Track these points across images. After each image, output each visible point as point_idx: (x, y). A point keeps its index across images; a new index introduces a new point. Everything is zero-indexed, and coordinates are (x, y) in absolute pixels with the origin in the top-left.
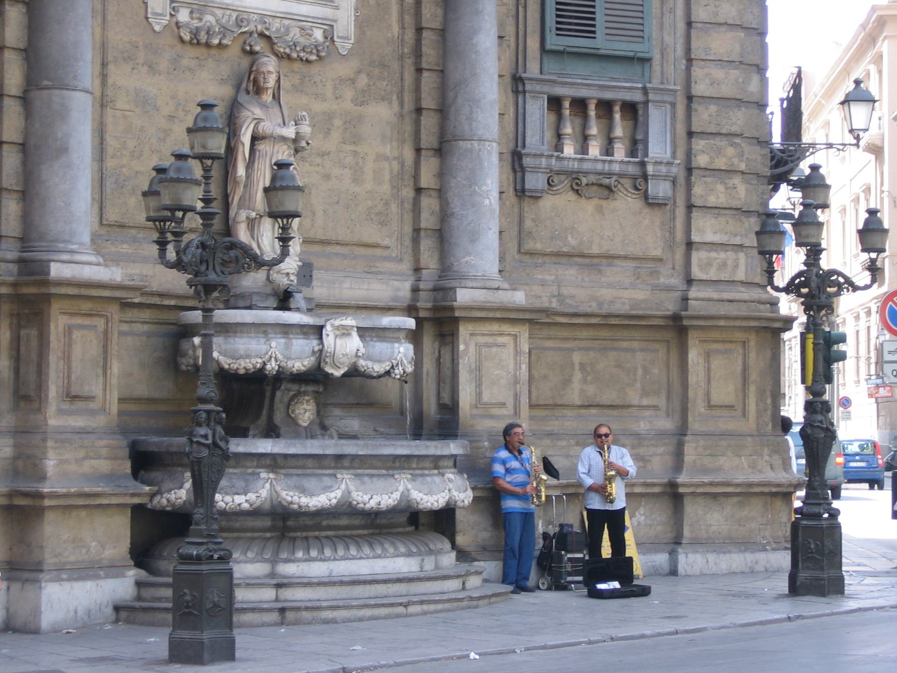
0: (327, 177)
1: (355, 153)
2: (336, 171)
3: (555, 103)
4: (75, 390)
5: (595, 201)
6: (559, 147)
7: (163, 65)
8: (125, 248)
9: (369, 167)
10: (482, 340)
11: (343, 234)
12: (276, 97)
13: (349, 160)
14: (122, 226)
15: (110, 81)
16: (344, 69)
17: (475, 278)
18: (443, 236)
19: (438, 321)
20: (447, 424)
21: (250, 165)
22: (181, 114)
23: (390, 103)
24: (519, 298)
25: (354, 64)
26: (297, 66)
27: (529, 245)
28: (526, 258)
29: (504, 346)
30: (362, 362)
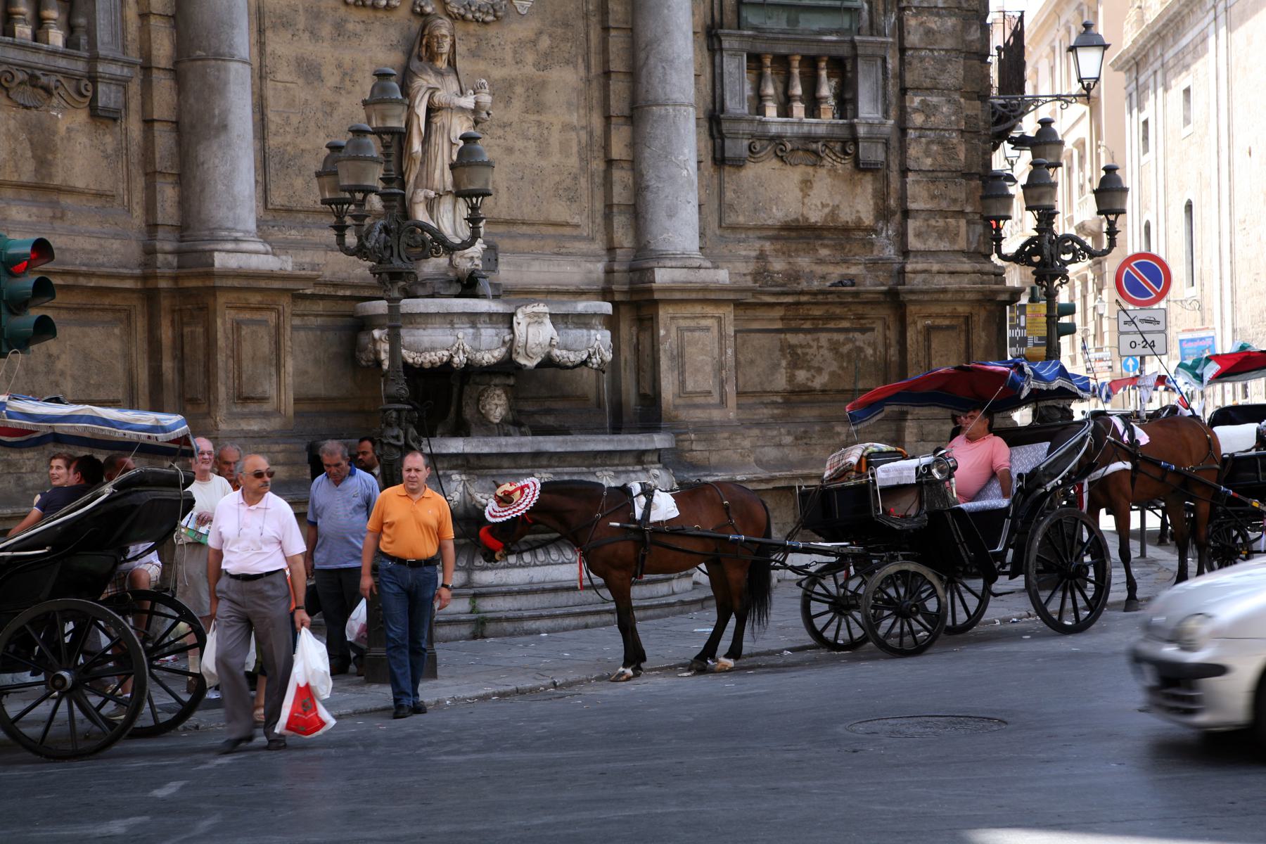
0: (510, 150)
1: (539, 123)
2: (520, 144)
3: (755, 60)
4: (246, 391)
5: (801, 169)
6: (760, 110)
7: (326, 30)
8: (294, 234)
9: (555, 138)
10: (683, 323)
11: (528, 212)
12: (452, 64)
13: (533, 130)
14: (289, 210)
15: (269, 49)
16: (522, 30)
17: (674, 257)
18: (637, 213)
19: (635, 304)
20: (650, 414)
21: (426, 141)
22: (348, 84)
23: (575, 67)
24: (722, 276)
25: (535, 24)
26: (472, 28)
27: (731, 219)
28: (727, 234)
29: (708, 329)
30: (556, 352)
